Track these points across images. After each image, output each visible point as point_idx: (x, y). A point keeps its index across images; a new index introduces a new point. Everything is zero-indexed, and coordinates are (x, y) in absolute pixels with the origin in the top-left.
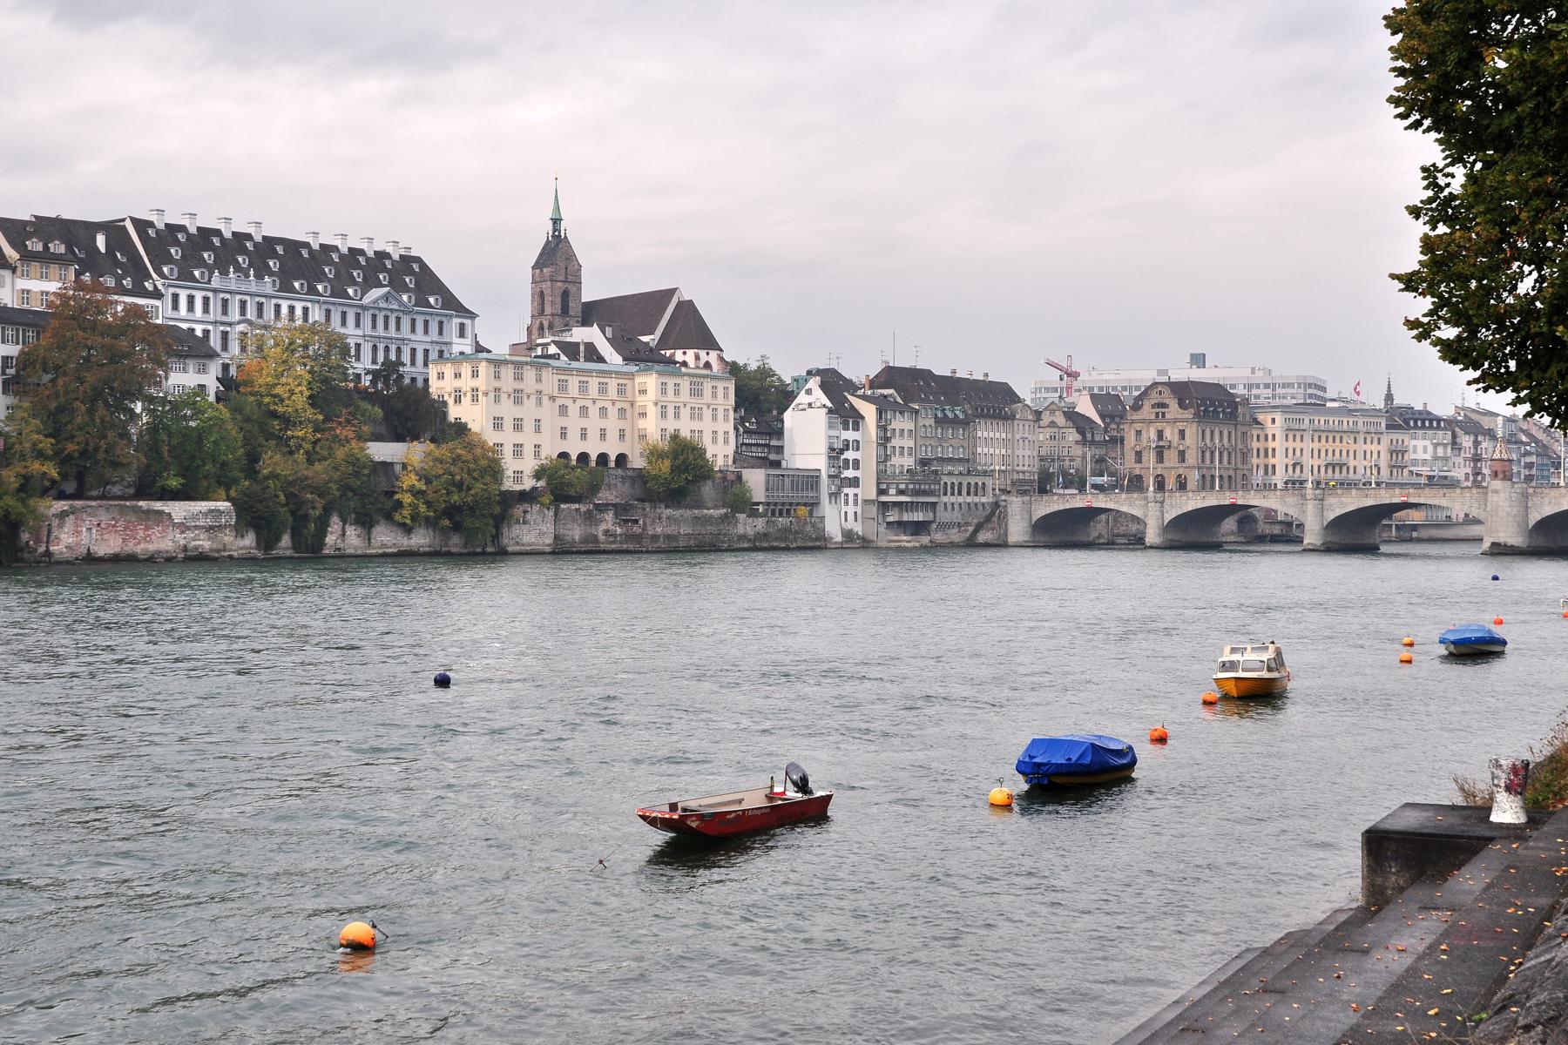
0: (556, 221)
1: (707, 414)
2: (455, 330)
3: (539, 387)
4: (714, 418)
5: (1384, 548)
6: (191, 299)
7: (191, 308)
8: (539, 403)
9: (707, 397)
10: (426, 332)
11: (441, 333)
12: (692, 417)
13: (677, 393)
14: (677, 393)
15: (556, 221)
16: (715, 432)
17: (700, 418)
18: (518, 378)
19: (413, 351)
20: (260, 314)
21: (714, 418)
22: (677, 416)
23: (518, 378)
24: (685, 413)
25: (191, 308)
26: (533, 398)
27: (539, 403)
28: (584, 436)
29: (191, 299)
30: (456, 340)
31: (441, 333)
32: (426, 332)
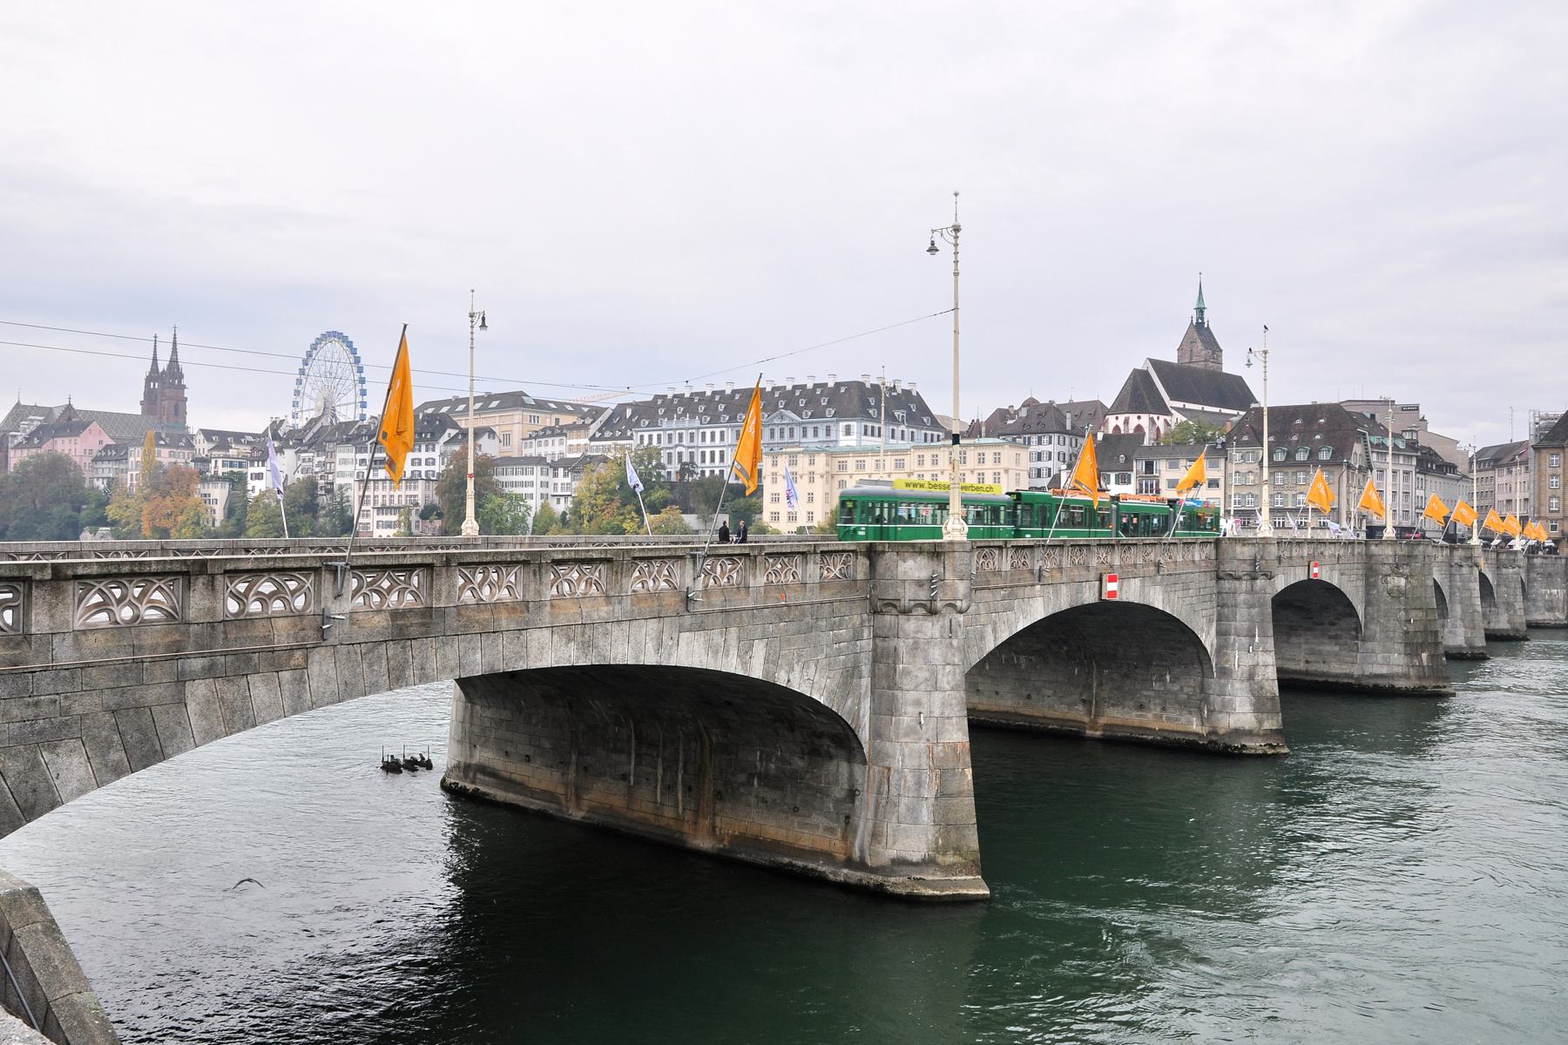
0: (1201, 311)
3: (812, 468)
6: (713, 434)
8: (812, 480)
10: (816, 435)
11: (828, 434)
15: (1201, 311)
18: (793, 463)
20: (692, 440)
23: (793, 463)
26: (806, 478)
27: (812, 480)
29: (713, 434)
30: (842, 436)
31: (828, 434)
32: (816, 435)
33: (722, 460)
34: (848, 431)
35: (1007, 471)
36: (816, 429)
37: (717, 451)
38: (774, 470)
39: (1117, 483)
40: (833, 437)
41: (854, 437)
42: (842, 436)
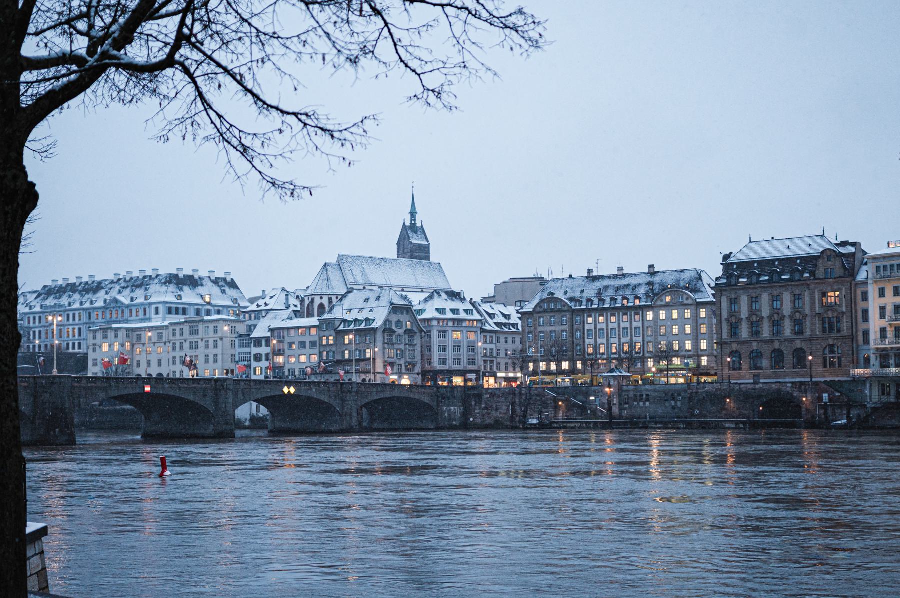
0: (413, 214)
1: (202, 344)
2: (153, 311)
4: (207, 346)
5: (238, 433)
7: (74, 319)
9: (201, 334)
11: (145, 314)
12: (191, 348)
13: (182, 334)
14: (182, 334)
15: (413, 214)
16: (207, 356)
17: (197, 347)
19: (34, 332)
21: (207, 346)
22: (182, 348)
24: (186, 345)
25: (74, 319)
28: (160, 364)
30: (153, 316)
31: (145, 314)
33: (80, 335)
34: (157, 312)
35: (221, 339)
36: (138, 312)
37: (77, 328)
38: (94, 341)
39: (255, 346)
40: (148, 316)
41: (160, 315)
42: (153, 316)
